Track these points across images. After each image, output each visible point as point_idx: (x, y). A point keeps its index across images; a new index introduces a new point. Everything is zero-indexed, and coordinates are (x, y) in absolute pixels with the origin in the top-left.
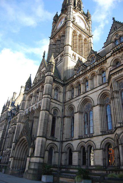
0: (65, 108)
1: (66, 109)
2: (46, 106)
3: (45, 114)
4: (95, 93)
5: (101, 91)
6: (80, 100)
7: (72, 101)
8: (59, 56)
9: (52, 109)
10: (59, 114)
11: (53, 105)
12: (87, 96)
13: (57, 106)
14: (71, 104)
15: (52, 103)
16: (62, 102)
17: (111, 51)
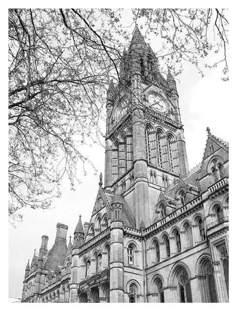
0: (147, 279)
1: (150, 281)
2: (118, 282)
3: (119, 296)
4: (191, 257)
5: (200, 254)
6: (171, 267)
7: (157, 267)
8: (127, 177)
9: (128, 283)
10: (139, 291)
11: (129, 276)
12: (181, 261)
13: (134, 277)
14: (157, 273)
15: (125, 274)
16: (142, 268)
17: (208, 190)
